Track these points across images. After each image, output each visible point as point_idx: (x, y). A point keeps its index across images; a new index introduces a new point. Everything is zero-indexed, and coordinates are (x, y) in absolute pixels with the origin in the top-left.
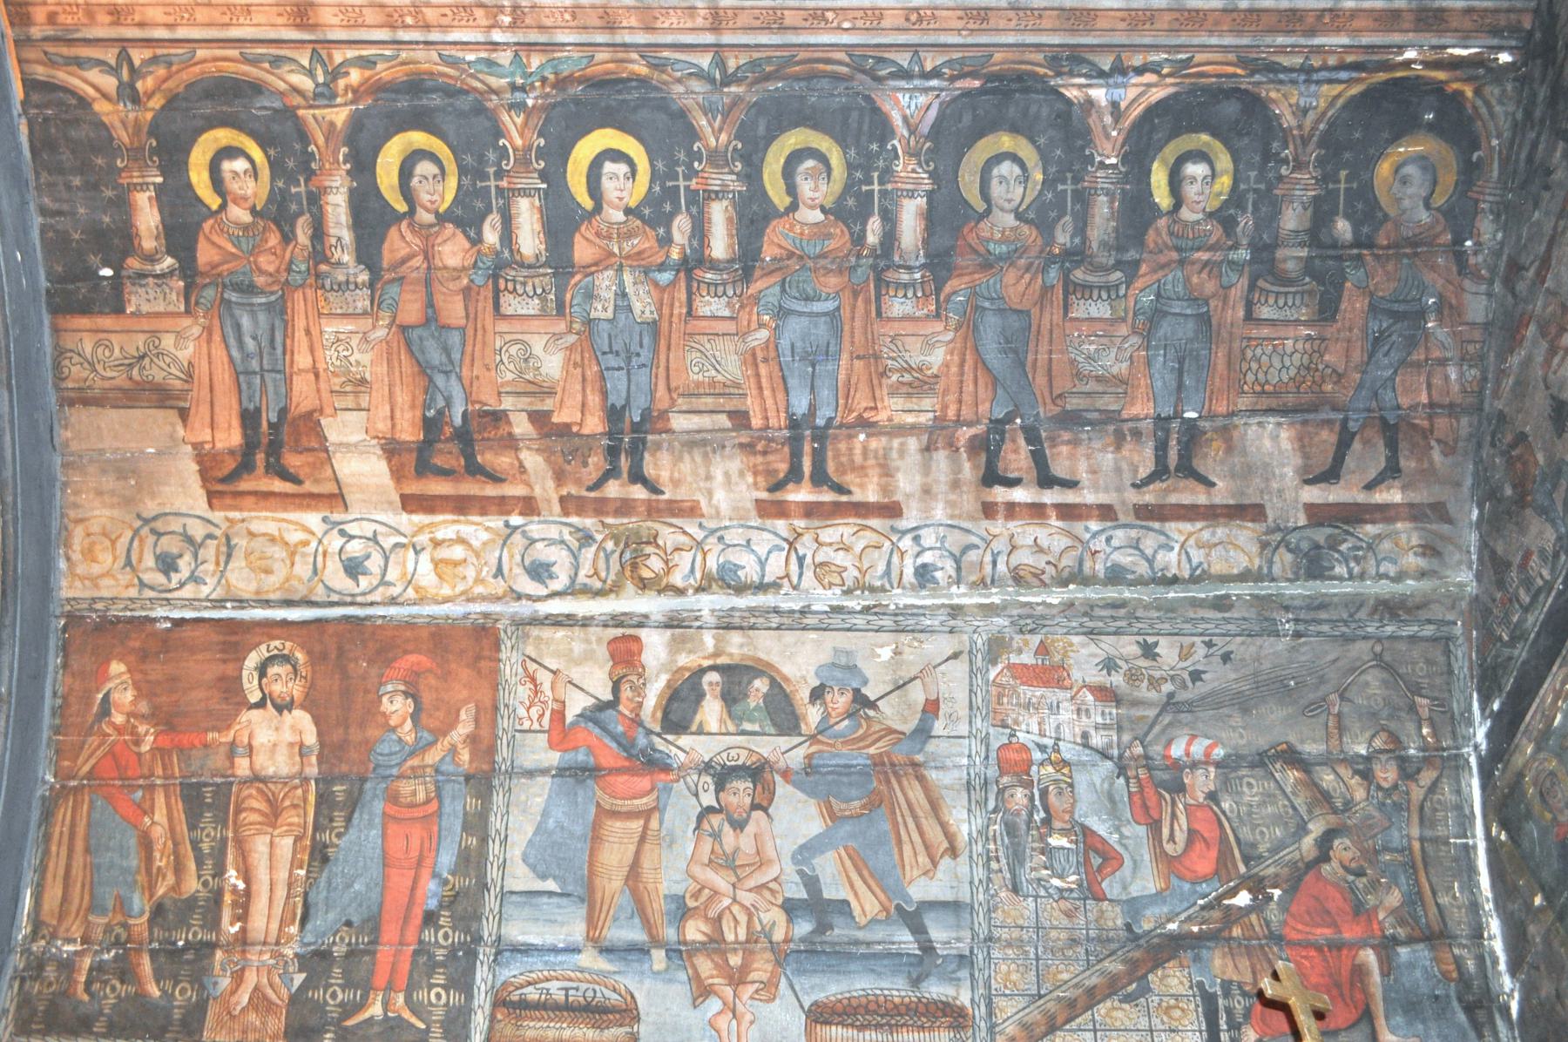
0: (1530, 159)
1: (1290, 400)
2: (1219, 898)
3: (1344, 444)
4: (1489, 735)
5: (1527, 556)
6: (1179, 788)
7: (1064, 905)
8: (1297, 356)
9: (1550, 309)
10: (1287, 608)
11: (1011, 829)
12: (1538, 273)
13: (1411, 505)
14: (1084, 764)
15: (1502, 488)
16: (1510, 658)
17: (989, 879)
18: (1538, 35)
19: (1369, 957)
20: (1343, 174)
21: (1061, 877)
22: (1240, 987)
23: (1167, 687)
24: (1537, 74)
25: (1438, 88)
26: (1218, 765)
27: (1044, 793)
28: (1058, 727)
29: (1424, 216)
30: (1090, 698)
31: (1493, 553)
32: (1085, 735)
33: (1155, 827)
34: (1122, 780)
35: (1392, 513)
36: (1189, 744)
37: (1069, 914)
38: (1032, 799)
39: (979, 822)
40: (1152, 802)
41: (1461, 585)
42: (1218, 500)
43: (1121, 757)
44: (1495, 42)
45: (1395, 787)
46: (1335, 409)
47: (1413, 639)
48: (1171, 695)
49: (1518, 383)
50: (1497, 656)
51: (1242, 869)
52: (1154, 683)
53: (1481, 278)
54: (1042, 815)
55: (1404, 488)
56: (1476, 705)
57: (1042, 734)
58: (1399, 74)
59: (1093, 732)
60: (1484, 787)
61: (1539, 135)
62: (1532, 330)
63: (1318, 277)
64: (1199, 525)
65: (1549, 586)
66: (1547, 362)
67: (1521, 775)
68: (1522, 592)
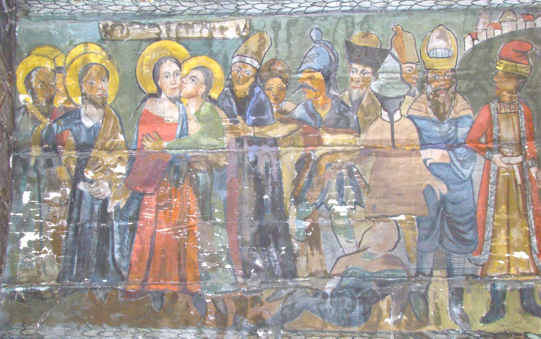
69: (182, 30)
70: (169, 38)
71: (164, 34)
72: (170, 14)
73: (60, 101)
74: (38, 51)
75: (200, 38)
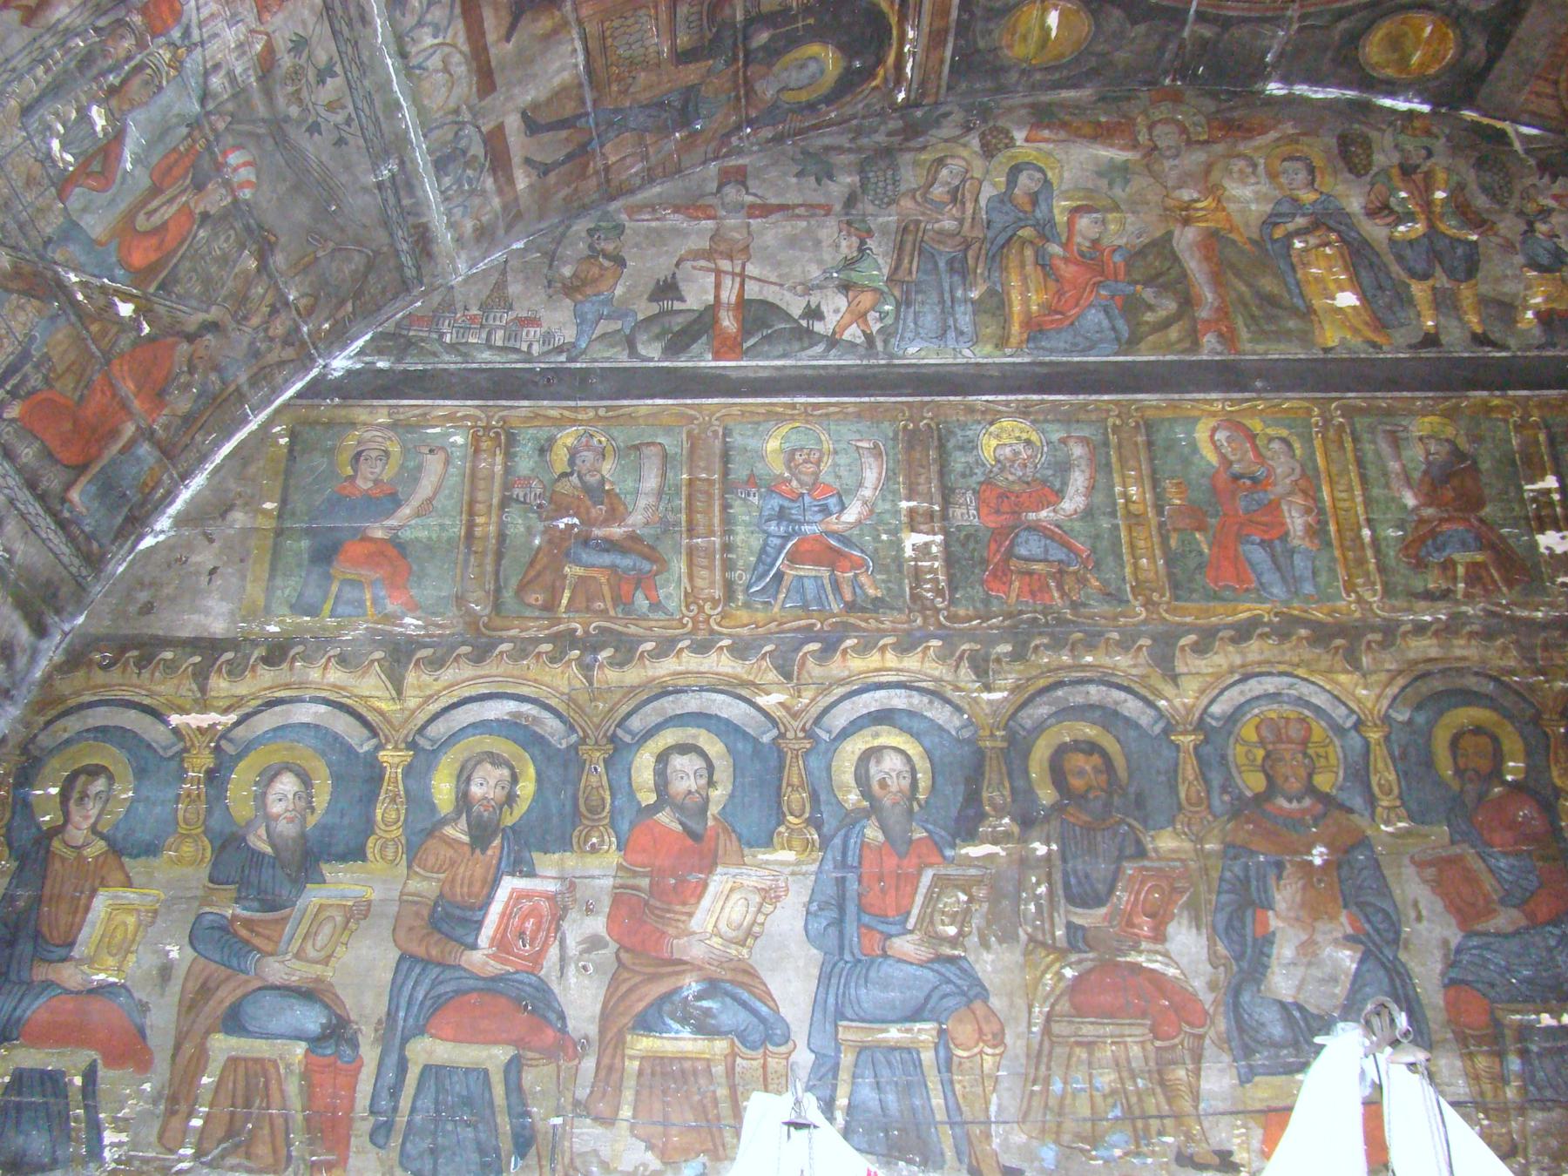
0: (827, 149)
1: (600, 63)
2: (117, 292)
3: (562, 124)
4: (350, 373)
5: (533, 321)
6: (199, 187)
7: (37, 170)
8: (642, 50)
9: (737, 236)
10: (402, 163)
11: (86, 60)
12: (752, 206)
13: (516, 199)
14: (185, 86)
15: (565, 263)
16: (435, 354)
17: (20, 78)
18: (919, 114)
19: (129, 429)
20: (811, 21)
21: (64, 147)
22: (50, 370)
23: (294, 111)
24: (892, 125)
25: (880, 61)
26: (236, 201)
27: (139, 68)
28: (216, 35)
29: (770, 94)
30: (259, 47)
31: (500, 286)
32: (217, 67)
33: (156, 190)
34: (184, 131)
35: (506, 189)
36: (245, 164)
37: (30, 182)
38: (129, 59)
39: (77, 21)
40: (177, 171)
41: (455, 270)
42: (493, 51)
43: (208, 114)
44: (915, 86)
45: (272, 339)
46: (595, 102)
47: (401, 267)
48: (287, 119)
49: (656, 231)
50: (423, 340)
51: (151, 290)
52: (296, 97)
53: (720, 149)
54: (117, 82)
55: (531, 186)
56: (360, 343)
57: (200, 25)
58: (895, 32)
59: (223, 72)
60: (300, 395)
61: (850, 150)
62: (710, 224)
63: (718, 38)
64: (465, 48)
65: (528, 356)
66: (697, 255)
67: (353, 425)
68: (500, 333)
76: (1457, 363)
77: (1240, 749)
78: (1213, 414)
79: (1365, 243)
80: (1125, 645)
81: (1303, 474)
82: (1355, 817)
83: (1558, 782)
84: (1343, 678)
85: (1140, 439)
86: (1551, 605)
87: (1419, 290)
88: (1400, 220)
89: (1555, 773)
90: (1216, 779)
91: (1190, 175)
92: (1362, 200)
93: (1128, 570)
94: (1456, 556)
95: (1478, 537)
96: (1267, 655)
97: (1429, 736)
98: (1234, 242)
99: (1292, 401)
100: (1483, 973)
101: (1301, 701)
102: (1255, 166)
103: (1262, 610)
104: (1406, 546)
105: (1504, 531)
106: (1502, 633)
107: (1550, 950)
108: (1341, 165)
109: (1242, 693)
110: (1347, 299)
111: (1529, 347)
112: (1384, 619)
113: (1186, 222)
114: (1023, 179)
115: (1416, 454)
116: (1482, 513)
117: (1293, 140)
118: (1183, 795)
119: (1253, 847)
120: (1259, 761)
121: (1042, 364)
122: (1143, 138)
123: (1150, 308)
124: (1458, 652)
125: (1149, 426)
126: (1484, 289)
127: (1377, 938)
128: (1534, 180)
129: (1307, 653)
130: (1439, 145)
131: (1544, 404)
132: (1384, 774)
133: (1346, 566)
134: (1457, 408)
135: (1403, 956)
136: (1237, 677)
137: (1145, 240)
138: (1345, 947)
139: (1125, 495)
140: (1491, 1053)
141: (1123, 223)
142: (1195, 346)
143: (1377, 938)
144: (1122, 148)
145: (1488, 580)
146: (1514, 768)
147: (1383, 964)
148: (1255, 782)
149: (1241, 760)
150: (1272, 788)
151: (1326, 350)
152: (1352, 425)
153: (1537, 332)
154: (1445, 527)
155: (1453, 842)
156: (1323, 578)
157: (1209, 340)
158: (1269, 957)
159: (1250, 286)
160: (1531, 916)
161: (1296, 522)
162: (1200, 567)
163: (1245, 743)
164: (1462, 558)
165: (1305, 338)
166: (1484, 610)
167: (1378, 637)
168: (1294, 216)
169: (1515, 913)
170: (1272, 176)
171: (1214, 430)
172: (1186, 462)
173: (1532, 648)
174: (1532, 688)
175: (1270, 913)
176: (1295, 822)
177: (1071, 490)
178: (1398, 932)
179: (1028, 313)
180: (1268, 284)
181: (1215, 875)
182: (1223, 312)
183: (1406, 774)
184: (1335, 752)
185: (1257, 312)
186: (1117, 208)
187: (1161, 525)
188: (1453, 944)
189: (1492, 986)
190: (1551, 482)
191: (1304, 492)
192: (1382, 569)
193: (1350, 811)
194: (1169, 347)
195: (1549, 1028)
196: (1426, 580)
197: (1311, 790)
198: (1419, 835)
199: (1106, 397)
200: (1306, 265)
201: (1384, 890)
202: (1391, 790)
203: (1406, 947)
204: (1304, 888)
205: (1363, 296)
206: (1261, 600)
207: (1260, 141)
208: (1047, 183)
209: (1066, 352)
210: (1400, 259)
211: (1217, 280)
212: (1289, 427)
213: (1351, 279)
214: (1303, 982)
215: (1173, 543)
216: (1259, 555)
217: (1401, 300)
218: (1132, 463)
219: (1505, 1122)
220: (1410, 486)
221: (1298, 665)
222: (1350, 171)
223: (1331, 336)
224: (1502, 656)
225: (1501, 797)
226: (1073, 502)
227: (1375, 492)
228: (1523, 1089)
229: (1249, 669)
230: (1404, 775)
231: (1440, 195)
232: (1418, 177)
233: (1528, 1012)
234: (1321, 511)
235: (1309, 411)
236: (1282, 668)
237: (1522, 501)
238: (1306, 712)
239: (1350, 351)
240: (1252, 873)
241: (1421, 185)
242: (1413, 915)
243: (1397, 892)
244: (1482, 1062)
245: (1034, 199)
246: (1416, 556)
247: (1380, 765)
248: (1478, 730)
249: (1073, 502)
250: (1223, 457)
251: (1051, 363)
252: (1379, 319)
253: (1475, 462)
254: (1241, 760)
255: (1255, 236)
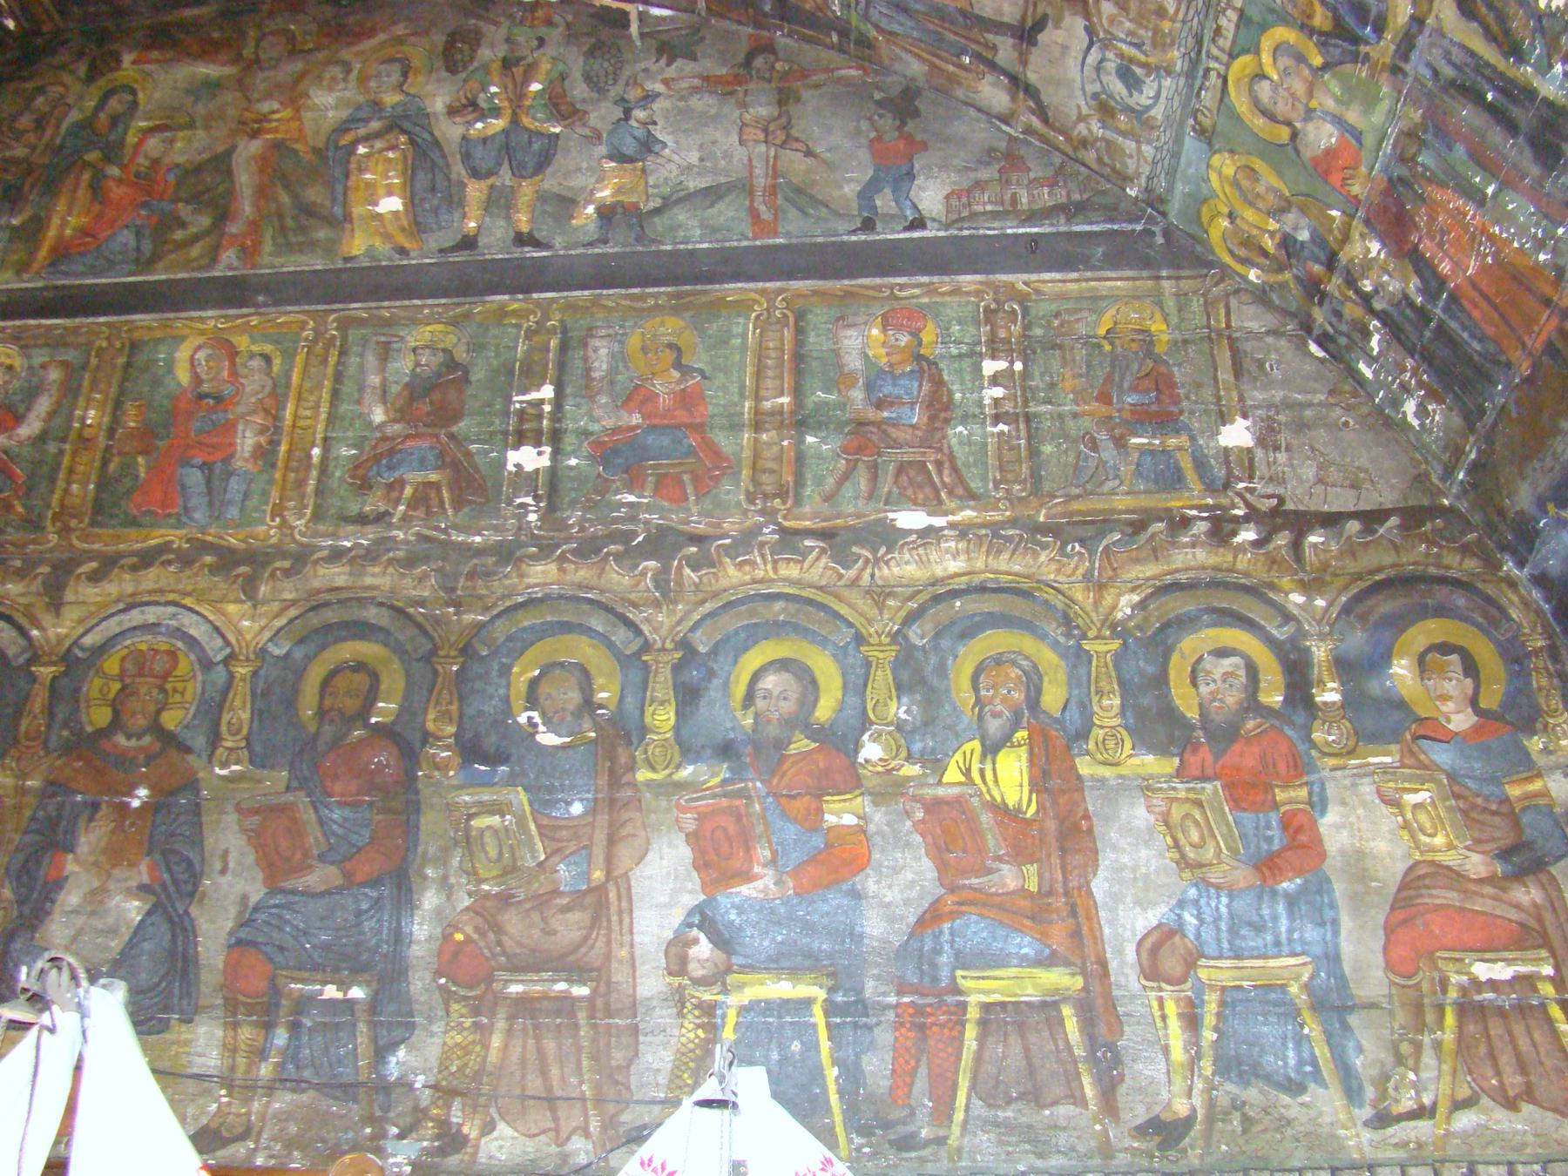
69: (1221, 42)
70: (1228, 66)
71: (1222, 69)
72: (1199, 42)
73: (1269, 244)
74: (1205, 220)
75: (1238, 27)
76: (485, 266)
77: (98, 682)
78: (202, 332)
79: (436, 143)
80: (21, 574)
81: (273, 394)
82: (191, 759)
83: (430, 726)
84: (231, 608)
85: (121, 360)
86: (496, 529)
87: (475, 191)
88: (482, 117)
89: (431, 716)
90: (62, 711)
91: (278, 86)
92: (448, 99)
93: (57, 496)
94: (409, 476)
95: (441, 455)
96: (163, 583)
97: (300, 673)
98: (295, 151)
99: (289, 315)
100: (275, 935)
101: (180, 633)
102: (349, 71)
103: (175, 536)
104: (356, 466)
105: (473, 447)
106: (427, 559)
107: (359, 913)
108: (439, 63)
109: (120, 623)
110: (391, 204)
111: (575, 245)
112: (301, 545)
113: (254, 135)
114: (114, 104)
115: (403, 366)
116: (454, 429)
117: (400, 41)
118: (23, 728)
119: (73, 785)
120: (111, 696)
121: (56, 288)
122: (248, 52)
123: (183, 225)
124: (369, 581)
125: (134, 346)
126: (546, 185)
127: (172, 889)
128: (649, 63)
129: (204, 582)
130: (555, 34)
131: (571, 307)
132: (240, 712)
133: (283, 489)
134: (467, 316)
135: (194, 911)
136: (121, 606)
137: (205, 156)
138: (137, 898)
139: (83, 419)
140: (255, 1024)
141: (190, 140)
142: (214, 260)
143: (172, 889)
144: (224, 64)
145: (435, 502)
146: (385, 709)
147: (171, 921)
148: (101, 716)
149: (95, 693)
150: (116, 724)
151: (347, 259)
152: (344, 338)
153: (592, 227)
154: (409, 443)
155: (288, 789)
156: (250, 504)
157: (229, 256)
158: (53, 902)
159: (295, 196)
160: (348, 875)
161: (247, 441)
162: (129, 492)
163: (105, 675)
164: (414, 477)
165: (330, 248)
166: (418, 535)
167: (287, 564)
168: (367, 121)
169: (332, 870)
170: (363, 80)
171: (199, 348)
172: (157, 382)
173: (456, 577)
174: (437, 621)
175: (70, 856)
176: (124, 761)
177: (32, 416)
178: (196, 886)
179: (60, 236)
180: (315, 194)
181: (27, 813)
182: (255, 226)
183: (261, 712)
184: (193, 689)
185: (290, 223)
186: (191, 125)
187: (108, 448)
188: (253, 900)
189: (281, 949)
190: (547, 392)
191: (267, 411)
192: (319, 492)
193: (188, 750)
194: (187, 265)
195: (332, 1002)
196: (364, 503)
197: (156, 728)
198: (252, 779)
199: (102, 319)
200: (361, 170)
201: (197, 841)
202: (239, 731)
203: (201, 901)
204: (113, 832)
205: (412, 202)
206: (179, 525)
207: (367, 45)
208: (134, 104)
209: (84, 275)
210: (467, 157)
211: (262, 192)
212: (276, 342)
213: (404, 184)
214: (80, 932)
215: (112, 467)
216: (194, 478)
217: (451, 203)
218: (102, 386)
219: (247, 1101)
220: (384, 402)
221: (189, 594)
222: (448, 69)
223: (358, 245)
224: (419, 587)
225: (361, 740)
226: (29, 429)
227: (344, 408)
228: (280, 1066)
229: (138, 599)
230: (258, 714)
231: (536, 87)
232: (518, 71)
233: (314, 982)
234: (278, 430)
235: (305, 323)
236: (171, 597)
237: (507, 413)
238: (180, 644)
239: (372, 258)
240: (66, 813)
241: (519, 79)
242: (218, 866)
243: (209, 842)
244: (246, 1033)
245: (115, 121)
246: (364, 479)
247: (238, 703)
248: (360, 666)
249: (29, 429)
250: (197, 380)
251: (64, 287)
252: (417, 224)
253: (466, 372)
254: (95, 693)
255: (320, 144)
